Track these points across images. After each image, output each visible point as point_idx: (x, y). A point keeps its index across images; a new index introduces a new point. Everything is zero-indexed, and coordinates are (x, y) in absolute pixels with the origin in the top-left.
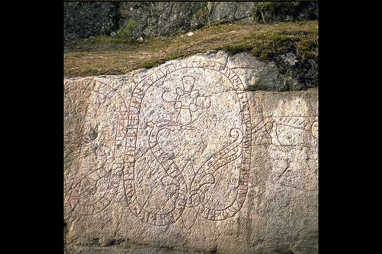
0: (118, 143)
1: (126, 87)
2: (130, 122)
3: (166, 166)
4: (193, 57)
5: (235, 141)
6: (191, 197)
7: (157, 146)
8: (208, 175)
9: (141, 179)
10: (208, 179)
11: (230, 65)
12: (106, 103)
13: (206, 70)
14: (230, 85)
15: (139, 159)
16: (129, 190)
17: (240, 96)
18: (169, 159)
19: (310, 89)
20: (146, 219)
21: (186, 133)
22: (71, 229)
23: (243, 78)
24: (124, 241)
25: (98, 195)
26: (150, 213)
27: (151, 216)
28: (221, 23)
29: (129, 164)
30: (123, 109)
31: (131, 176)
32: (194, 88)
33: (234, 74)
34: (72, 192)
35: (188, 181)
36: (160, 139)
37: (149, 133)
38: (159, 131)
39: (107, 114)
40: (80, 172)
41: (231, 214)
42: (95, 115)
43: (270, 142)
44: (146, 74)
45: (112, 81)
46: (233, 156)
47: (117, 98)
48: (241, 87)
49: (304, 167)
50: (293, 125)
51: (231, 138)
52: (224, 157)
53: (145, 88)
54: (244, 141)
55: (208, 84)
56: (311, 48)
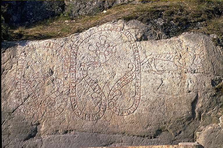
0: (66, 76)
1: (68, 44)
2: (71, 64)
3: (93, 87)
4: (105, 24)
5: (131, 70)
6: (109, 104)
7: (88, 76)
8: (118, 91)
9: (80, 95)
10: (117, 93)
11: (126, 27)
12: (57, 54)
13: (113, 31)
14: (127, 39)
15: (78, 85)
16: (74, 102)
18: (95, 83)
19: (172, 38)
20: (84, 118)
21: (103, 68)
22: (43, 126)
23: (134, 35)
24: (73, 130)
25: (56, 106)
26: (86, 114)
27: (87, 116)
28: (122, 5)
29: (72, 88)
30: (67, 57)
31: (74, 94)
32: (107, 42)
33: (128, 33)
34: (42, 105)
35: (106, 95)
36: (89, 72)
37: (82, 70)
38: (88, 68)
39: (58, 60)
40: (45, 94)
41: (132, 111)
42: (52, 61)
43: (151, 70)
44: (79, 36)
45: (60, 41)
46: (131, 79)
47: (63, 51)
48: (133, 39)
49: (171, 82)
50: (164, 59)
51: (129, 69)
52: (126, 79)
53: (79, 44)
54: (137, 70)
55: (114, 39)
56: (171, 14)
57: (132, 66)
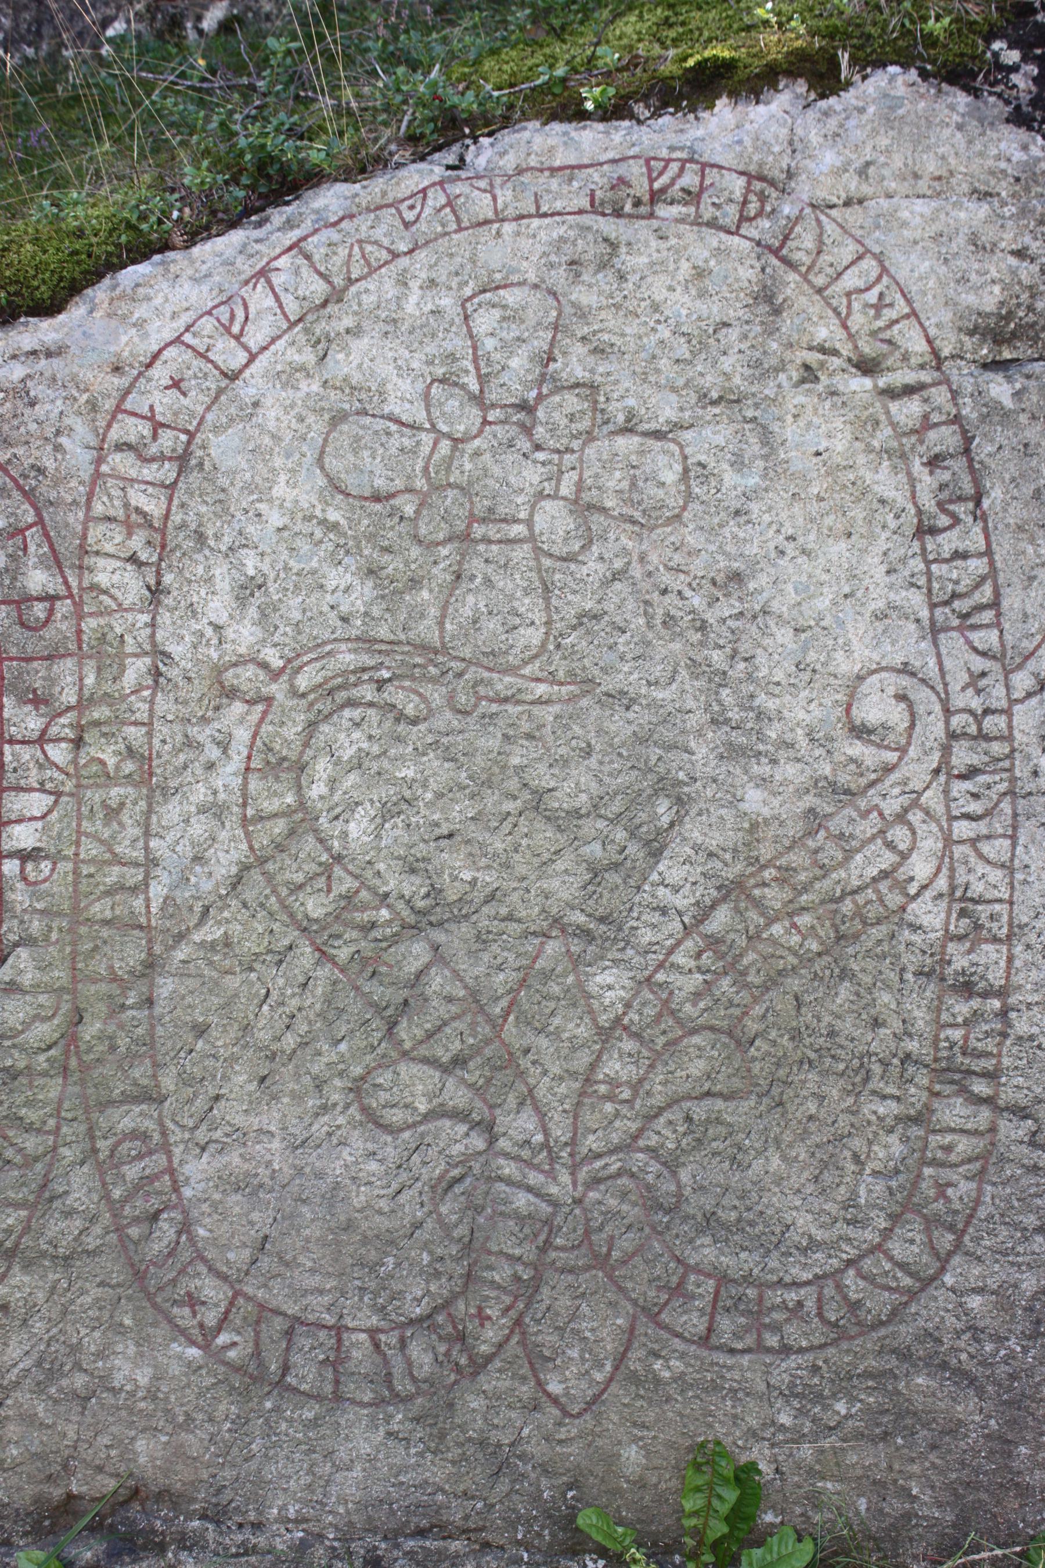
17: (909, 410)
31: (140, 1072)
46: (883, 886)
57: (897, 715)
